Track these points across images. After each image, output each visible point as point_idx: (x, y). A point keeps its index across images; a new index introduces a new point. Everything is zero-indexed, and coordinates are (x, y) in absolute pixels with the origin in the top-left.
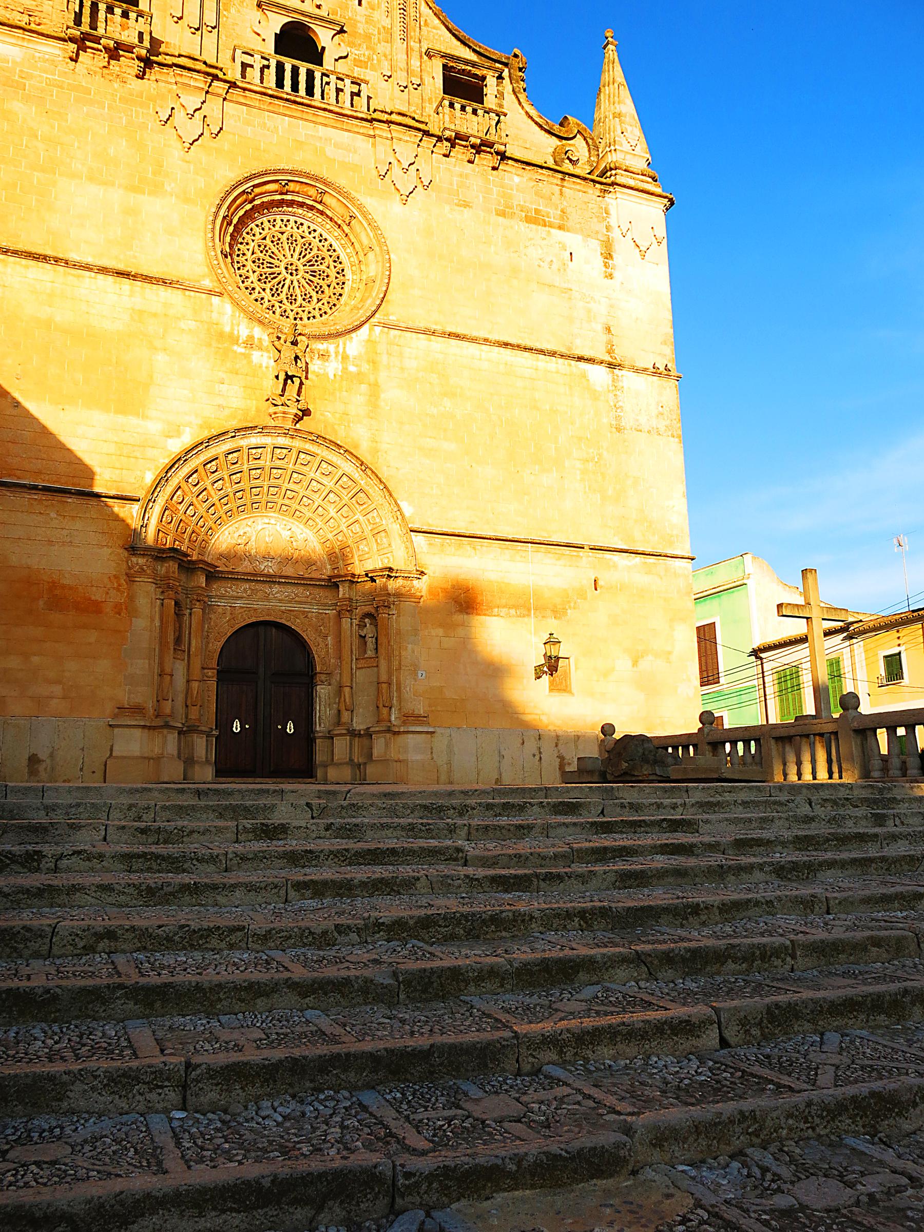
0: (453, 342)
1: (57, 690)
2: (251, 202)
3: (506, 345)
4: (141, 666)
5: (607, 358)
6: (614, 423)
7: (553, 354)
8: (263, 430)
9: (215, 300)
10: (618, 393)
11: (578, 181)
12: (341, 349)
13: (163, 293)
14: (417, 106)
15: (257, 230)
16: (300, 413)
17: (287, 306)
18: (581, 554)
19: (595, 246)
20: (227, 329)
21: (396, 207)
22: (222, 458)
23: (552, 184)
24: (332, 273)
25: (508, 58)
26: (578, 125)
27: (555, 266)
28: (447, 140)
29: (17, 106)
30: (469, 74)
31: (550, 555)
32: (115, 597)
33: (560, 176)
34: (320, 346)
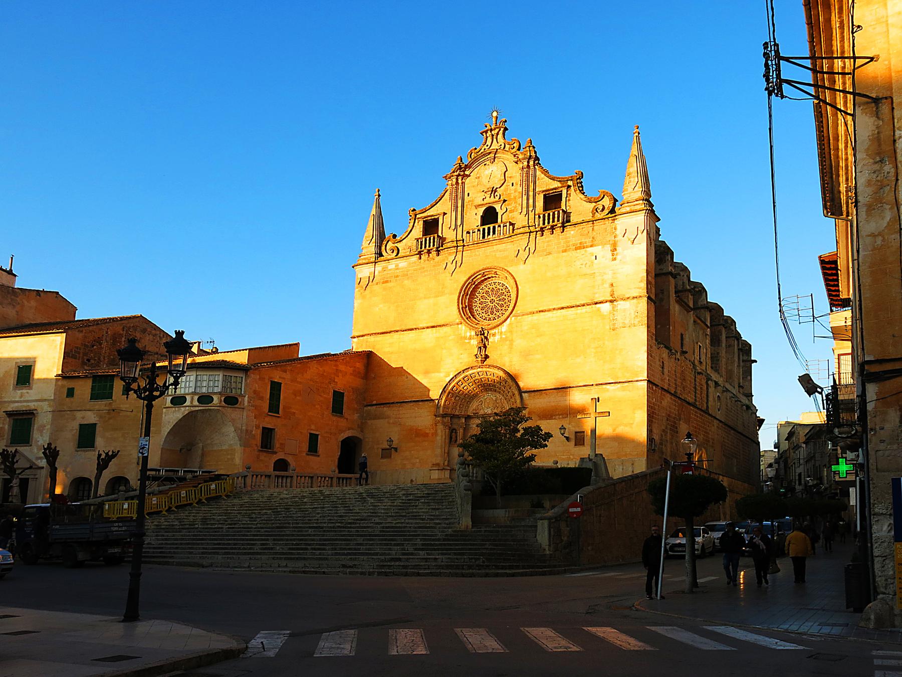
0: (542, 314)
2: (474, 284)
3: (563, 308)
5: (611, 298)
6: (612, 327)
9: (460, 326)
10: (615, 313)
11: (600, 221)
12: (500, 331)
13: (444, 328)
14: (532, 219)
15: (481, 291)
16: (484, 359)
17: (491, 316)
18: (592, 388)
19: (608, 248)
20: (463, 335)
21: (522, 267)
22: (462, 380)
23: (588, 227)
25: (572, 177)
26: (604, 192)
27: (587, 265)
28: (539, 231)
29: (406, 282)
30: (556, 192)
31: (578, 391)
32: (432, 431)
33: (591, 222)
34: (491, 332)
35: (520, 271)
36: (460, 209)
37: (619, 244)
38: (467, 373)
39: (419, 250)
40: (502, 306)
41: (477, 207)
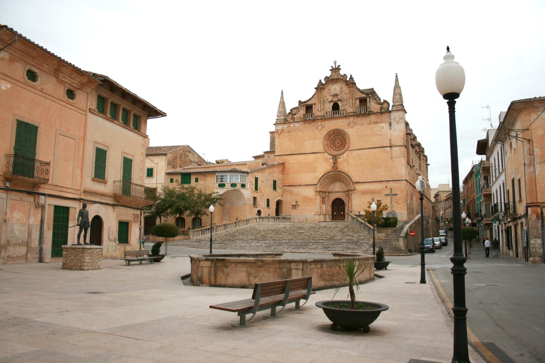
0: (361, 150)
1: (308, 210)
3: (370, 148)
4: (318, 207)
5: (390, 145)
7: (379, 148)
8: (332, 172)
9: (325, 153)
19: (388, 124)
21: (351, 130)
24: (344, 142)
35: (349, 131)
36: (322, 102)
37: (392, 123)
38: (329, 174)
39: (305, 119)
40: (342, 145)
41: (330, 102)
